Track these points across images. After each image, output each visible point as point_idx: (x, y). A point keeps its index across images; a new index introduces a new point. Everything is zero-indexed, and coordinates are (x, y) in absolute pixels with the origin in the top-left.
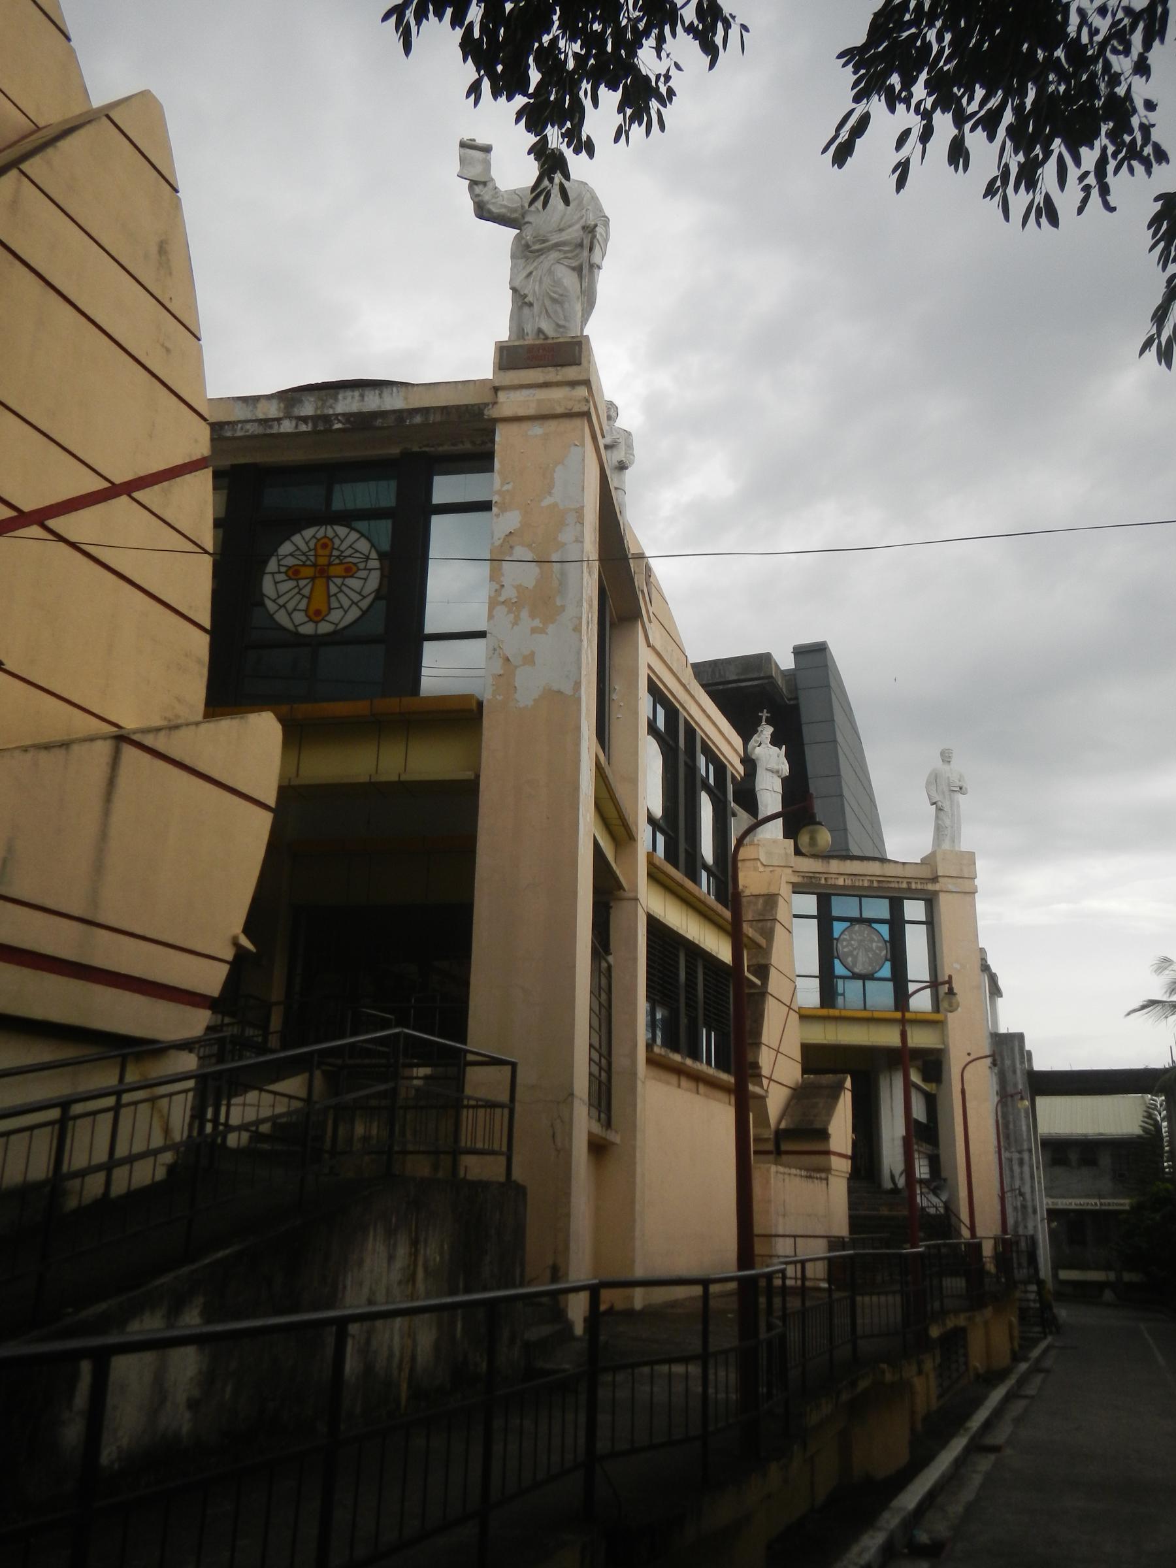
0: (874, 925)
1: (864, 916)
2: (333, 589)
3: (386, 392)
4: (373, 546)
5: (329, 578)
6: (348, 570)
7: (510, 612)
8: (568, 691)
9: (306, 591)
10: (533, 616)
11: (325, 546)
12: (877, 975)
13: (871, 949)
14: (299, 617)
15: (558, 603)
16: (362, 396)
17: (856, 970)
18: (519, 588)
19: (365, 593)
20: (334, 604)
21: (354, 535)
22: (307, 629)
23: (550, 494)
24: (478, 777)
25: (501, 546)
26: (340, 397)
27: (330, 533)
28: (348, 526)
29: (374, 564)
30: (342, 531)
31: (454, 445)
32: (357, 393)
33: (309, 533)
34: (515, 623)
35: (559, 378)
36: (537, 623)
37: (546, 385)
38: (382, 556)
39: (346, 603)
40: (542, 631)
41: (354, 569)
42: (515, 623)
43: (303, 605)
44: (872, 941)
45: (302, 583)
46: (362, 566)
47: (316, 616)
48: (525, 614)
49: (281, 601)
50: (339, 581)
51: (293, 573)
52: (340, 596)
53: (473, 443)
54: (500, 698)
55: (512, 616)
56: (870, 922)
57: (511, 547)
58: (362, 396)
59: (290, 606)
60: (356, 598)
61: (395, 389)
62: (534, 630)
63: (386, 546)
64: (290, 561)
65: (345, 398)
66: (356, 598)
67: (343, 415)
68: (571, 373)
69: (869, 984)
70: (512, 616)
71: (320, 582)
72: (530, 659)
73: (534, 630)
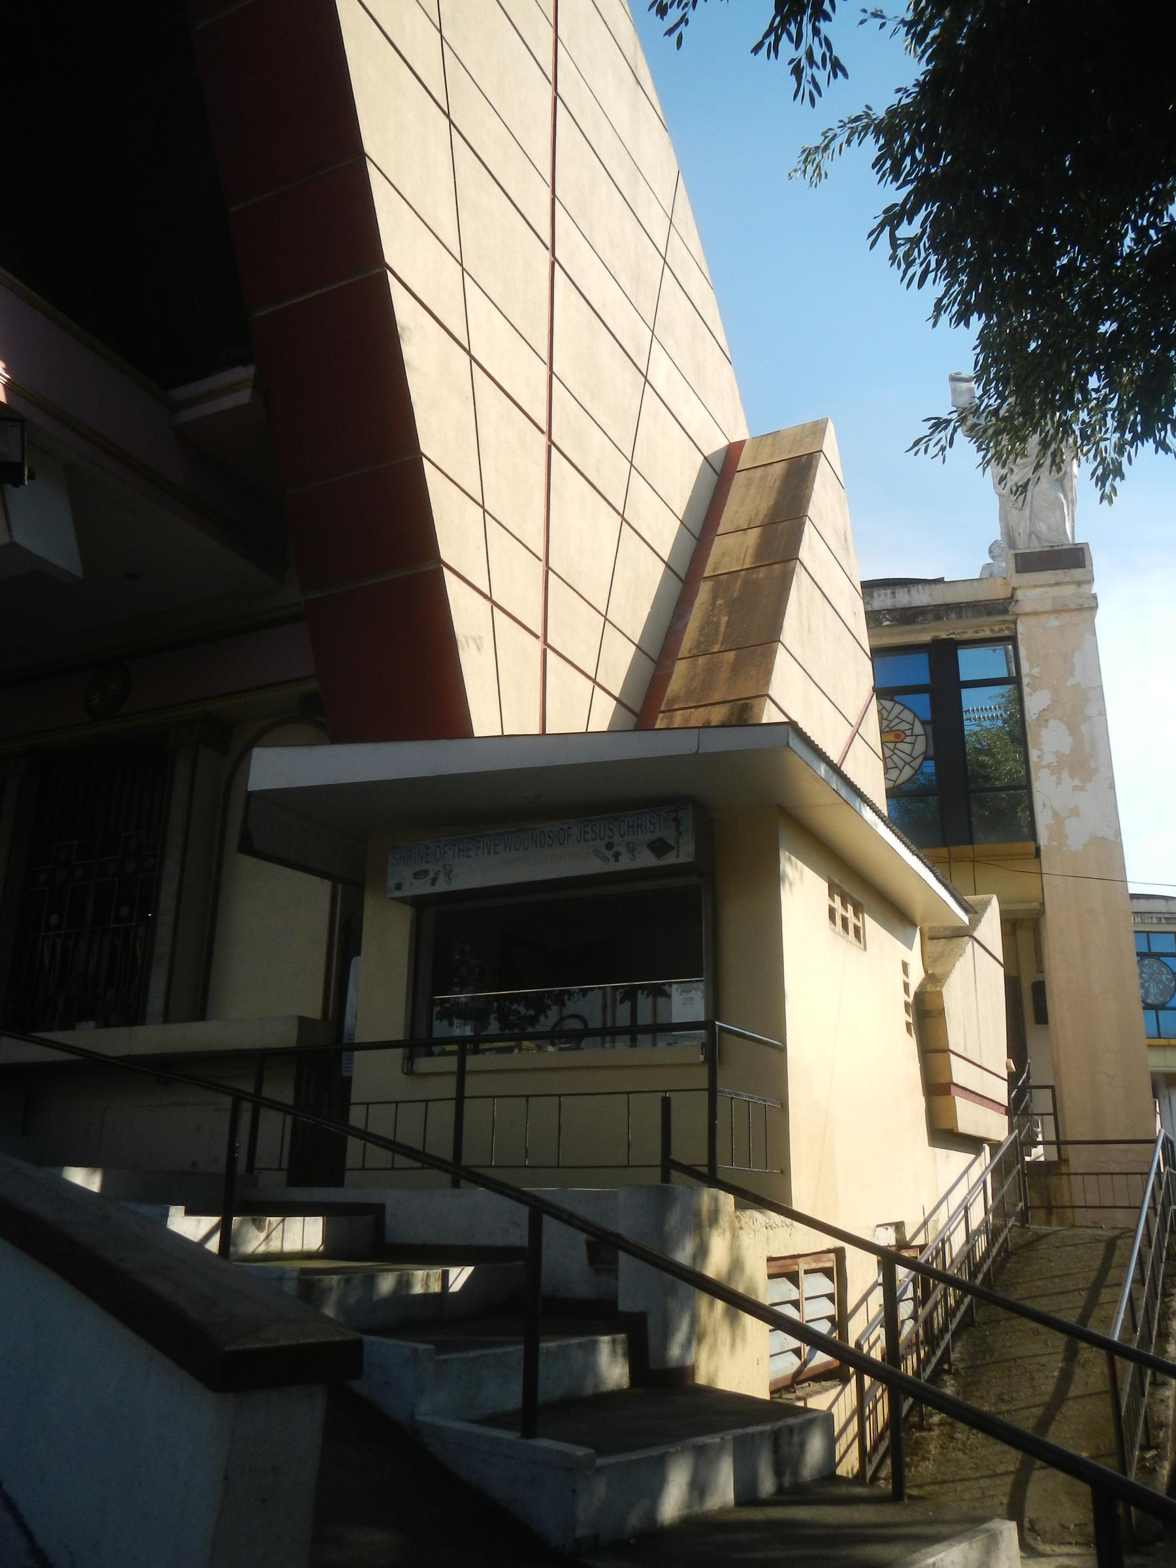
0: (1162, 959)
1: (1153, 950)
3: (914, 589)
4: (915, 716)
6: (897, 736)
7: (1052, 773)
8: (1112, 838)
10: (1072, 777)
12: (1169, 1005)
13: (1161, 982)
15: (1092, 765)
16: (893, 593)
17: (1149, 1001)
18: (1057, 753)
19: (915, 754)
21: (898, 708)
23: (1073, 676)
24: (1043, 904)
25: (1038, 719)
26: (875, 595)
28: (892, 700)
29: (918, 729)
31: (977, 632)
32: (889, 591)
34: (1059, 782)
35: (1068, 579)
36: (1077, 782)
37: (1057, 584)
38: (923, 723)
39: (900, 764)
40: (1082, 789)
41: (903, 736)
42: (1059, 782)
44: (1161, 973)
46: (908, 733)
48: (1065, 774)
52: (894, 757)
53: (992, 630)
54: (1055, 844)
55: (1054, 777)
56: (1158, 956)
57: (1046, 721)
58: (893, 593)
60: (908, 759)
61: (920, 587)
62: (1075, 788)
63: (928, 716)
65: (879, 596)
66: (908, 759)
67: (890, 611)
68: (1077, 573)
69: (1161, 1014)
70: (1054, 777)
72: (1075, 812)
73: (1075, 788)
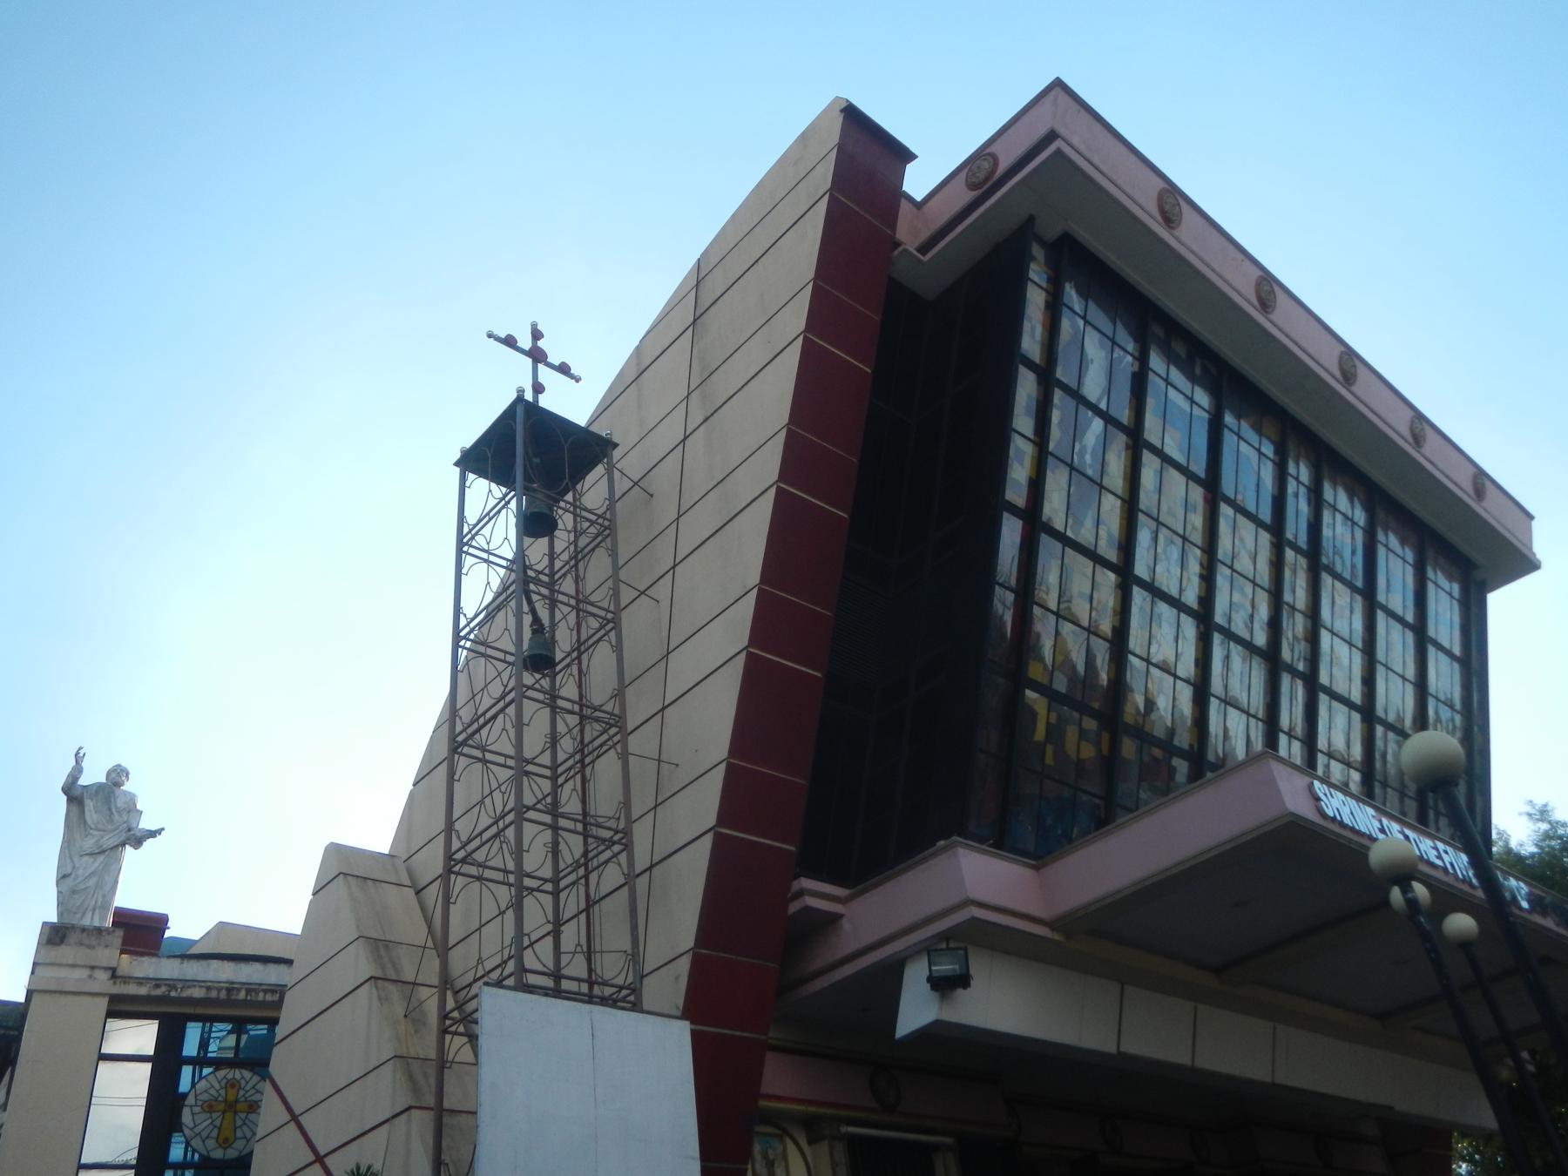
2: (239, 1123)
5: (236, 1113)
6: (251, 1106)
9: (218, 1123)
11: (233, 1086)
14: (211, 1143)
20: (239, 1134)
22: (218, 1154)
27: (238, 1076)
30: (247, 1074)
33: (221, 1074)
43: (215, 1133)
45: (215, 1115)
47: (225, 1143)
49: (197, 1130)
50: (243, 1116)
51: (209, 1107)
59: (204, 1134)
64: (205, 1097)
71: (229, 1115)
